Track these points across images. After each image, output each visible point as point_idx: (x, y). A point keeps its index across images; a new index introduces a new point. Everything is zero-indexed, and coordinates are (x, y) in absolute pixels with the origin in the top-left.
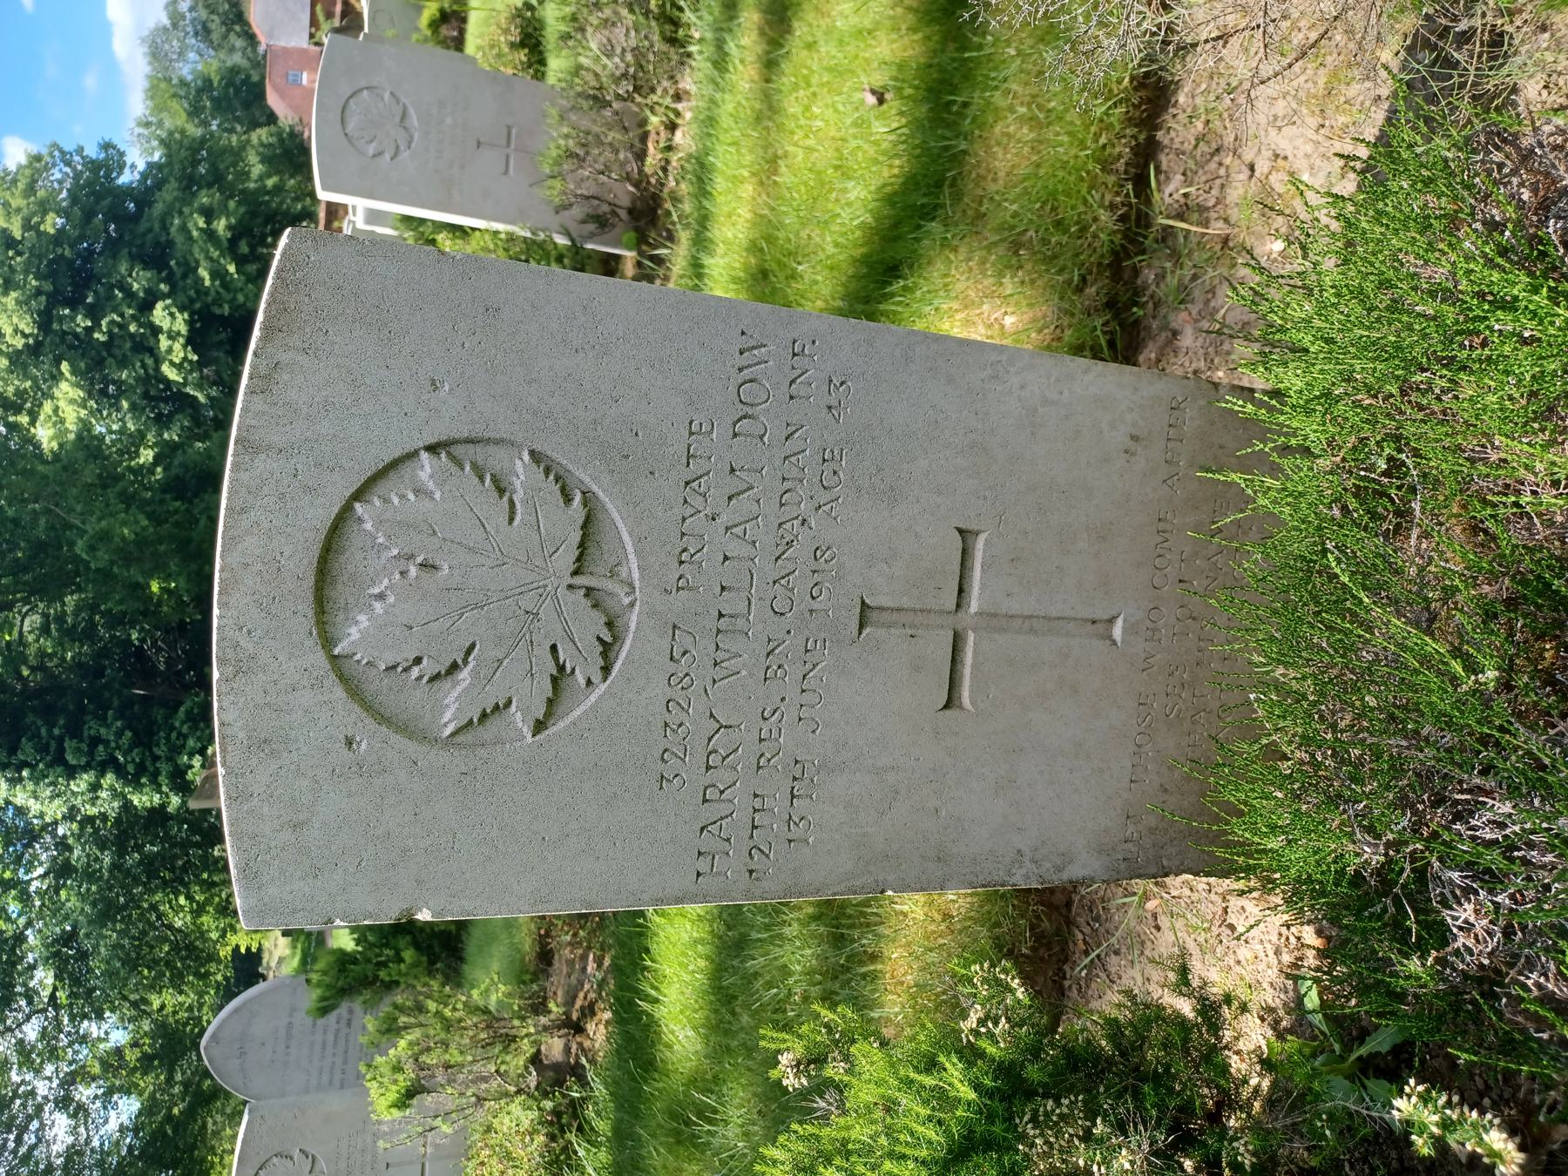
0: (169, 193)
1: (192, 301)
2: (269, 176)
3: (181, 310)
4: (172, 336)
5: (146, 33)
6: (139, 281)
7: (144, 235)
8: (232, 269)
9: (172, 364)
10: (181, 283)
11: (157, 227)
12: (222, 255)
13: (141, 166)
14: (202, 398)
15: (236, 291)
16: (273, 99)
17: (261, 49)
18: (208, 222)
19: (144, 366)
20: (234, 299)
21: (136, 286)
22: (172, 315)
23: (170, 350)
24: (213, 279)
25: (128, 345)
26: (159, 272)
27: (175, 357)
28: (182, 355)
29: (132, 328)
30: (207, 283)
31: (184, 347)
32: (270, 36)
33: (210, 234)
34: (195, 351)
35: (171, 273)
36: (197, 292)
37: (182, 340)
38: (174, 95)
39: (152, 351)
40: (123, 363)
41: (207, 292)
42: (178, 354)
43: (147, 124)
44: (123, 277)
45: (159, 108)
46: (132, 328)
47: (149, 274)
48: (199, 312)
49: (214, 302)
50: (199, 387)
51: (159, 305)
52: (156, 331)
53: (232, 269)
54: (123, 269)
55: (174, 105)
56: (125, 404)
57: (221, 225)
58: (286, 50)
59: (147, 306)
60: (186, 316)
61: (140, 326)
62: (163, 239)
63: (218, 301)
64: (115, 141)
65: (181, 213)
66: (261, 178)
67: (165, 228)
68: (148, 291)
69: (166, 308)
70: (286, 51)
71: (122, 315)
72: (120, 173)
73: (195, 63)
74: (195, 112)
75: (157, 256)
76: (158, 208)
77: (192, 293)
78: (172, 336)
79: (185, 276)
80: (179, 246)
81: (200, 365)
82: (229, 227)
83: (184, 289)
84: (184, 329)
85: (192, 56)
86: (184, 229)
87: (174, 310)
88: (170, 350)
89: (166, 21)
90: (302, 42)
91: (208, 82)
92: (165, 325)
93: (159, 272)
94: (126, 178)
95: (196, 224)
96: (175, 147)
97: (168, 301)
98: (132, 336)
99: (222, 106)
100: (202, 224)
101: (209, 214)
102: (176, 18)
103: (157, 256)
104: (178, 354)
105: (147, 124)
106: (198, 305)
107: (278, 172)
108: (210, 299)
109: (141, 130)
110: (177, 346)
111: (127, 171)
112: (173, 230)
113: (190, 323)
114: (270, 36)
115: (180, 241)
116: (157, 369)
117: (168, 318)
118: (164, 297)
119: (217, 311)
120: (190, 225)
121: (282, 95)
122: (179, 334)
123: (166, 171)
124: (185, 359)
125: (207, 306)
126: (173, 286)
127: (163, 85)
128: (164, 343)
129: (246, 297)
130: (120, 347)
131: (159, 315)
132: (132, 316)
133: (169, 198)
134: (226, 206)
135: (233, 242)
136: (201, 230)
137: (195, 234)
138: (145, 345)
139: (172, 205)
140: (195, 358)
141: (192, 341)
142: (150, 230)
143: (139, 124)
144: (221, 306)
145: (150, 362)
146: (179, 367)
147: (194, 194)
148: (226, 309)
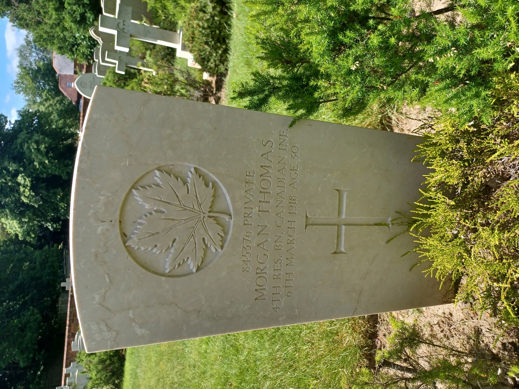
0: (23, 135)
1: (32, 173)
2: (60, 120)
3: (28, 177)
4: (25, 186)
5: (18, 47)
6: (12, 167)
7: (14, 149)
8: (47, 162)
9: (25, 196)
10: (28, 167)
11: (19, 147)
12: (43, 157)
13: (13, 122)
14: (36, 206)
15: (48, 169)
16: (61, 89)
17: (57, 75)
18: (38, 146)
19: (14, 196)
20: (48, 171)
21: (11, 169)
22: (25, 179)
23: (24, 191)
24: (39, 165)
25: (8, 190)
26: (20, 163)
27: (26, 195)
28: (28, 193)
29: (9, 184)
30: (38, 167)
31: (29, 190)
32: (60, 71)
33: (38, 150)
34: (33, 192)
35: (24, 162)
36: (34, 170)
37: (28, 188)
38: (28, 74)
39: (18, 191)
40: (6, 196)
41: (37, 170)
42: (27, 194)
43: (18, 83)
44: (7, 166)
45: (22, 77)
46: (9, 184)
47: (16, 165)
48: (35, 178)
49: (40, 173)
50: (36, 202)
51: (20, 175)
52: (19, 184)
53: (47, 162)
54: (6, 163)
55: (28, 77)
56: (8, 211)
57: (42, 147)
58: (66, 75)
59: (15, 175)
60: (30, 179)
61: (13, 183)
62: (21, 151)
63: (42, 172)
64: (4, 114)
65: (28, 143)
66: (57, 121)
67: (22, 147)
68: (16, 170)
69: (22, 176)
70: (66, 76)
71: (6, 179)
72: (4, 126)
73: (34, 59)
74: (34, 79)
75: (19, 158)
76: (19, 141)
77: (32, 170)
78: (25, 186)
79: (29, 164)
80: (27, 154)
81: (37, 194)
82: (45, 148)
83: (29, 169)
84: (29, 184)
85: (34, 54)
86: (28, 148)
87: (25, 177)
88: (24, 191)
89: (25, 44)
90: (72, 73)
91: (39, 68)
92: (22, 182)
93: (20, 163)
94: (8, 126)
95: (33, 147)
96: (25, 117)
97: (23, 174)
98: (10, 186)
99: (44, 76)
100: (35, 147)
101: (37, 143)
102: (28, 43)
103: (19, 158)
104: (27, 194)
105: (18, 83)
106: (34, 175)
107: (64, 118)
108: (38, 172)
109: (16, 85)
110: (27, 190)
111: (8, 123)
112: (25, 148)
113: (31, 182)
114: (60, 71)
115: (27, 152)
116: (20, 199)
117: (23, 180)
118: (21, 172)
119: (41, 176)
120: (31, 147)
121: (65, 91)
122: (27, 185)
123: (22, 126)
124: (30, 194)
125: (38, 174)
126: (25, 168)
127: (23, 70)
128: (22, 189)
129: (52, 171)
130: (5, 190)
131: (20, 179)
132: (10, 180)
133: (23, 137)
134: (44, 138)
135: (47, 153)
136: (35, 149)
137: (33, 150)
138: (15, 189)
139: (24, 139)
140: (34, 194)
141: (33, 188)
142: (17, 148)
143: (15, 83)
144: (43, 174)
145: (16, 195)
146: (27, 197)
147: (31, 133)
148: (45, 176)
